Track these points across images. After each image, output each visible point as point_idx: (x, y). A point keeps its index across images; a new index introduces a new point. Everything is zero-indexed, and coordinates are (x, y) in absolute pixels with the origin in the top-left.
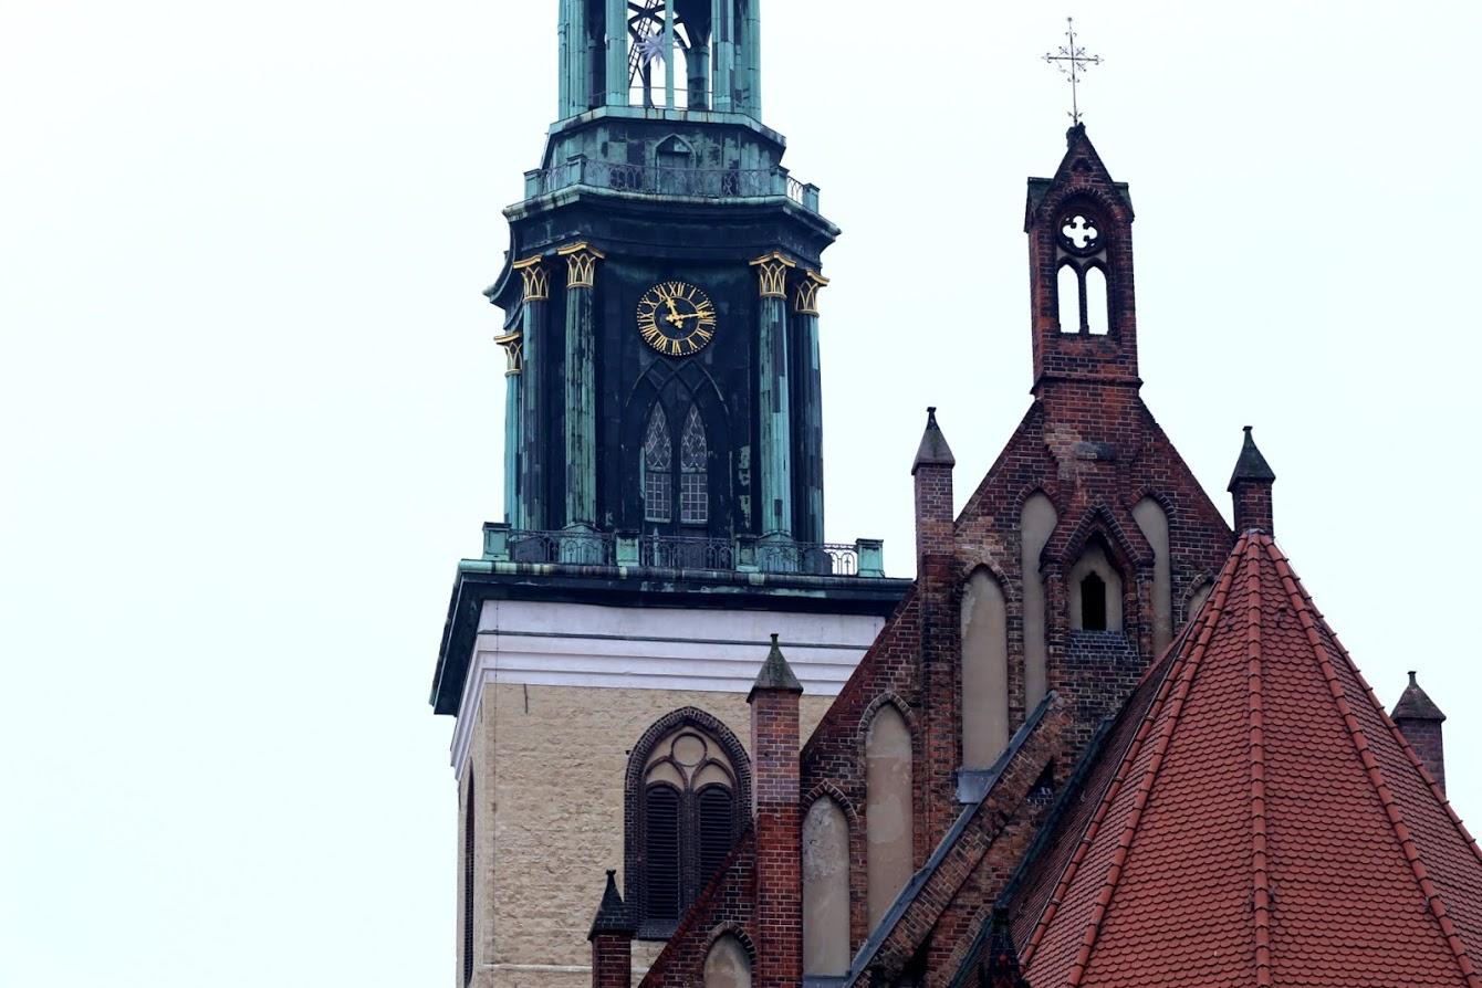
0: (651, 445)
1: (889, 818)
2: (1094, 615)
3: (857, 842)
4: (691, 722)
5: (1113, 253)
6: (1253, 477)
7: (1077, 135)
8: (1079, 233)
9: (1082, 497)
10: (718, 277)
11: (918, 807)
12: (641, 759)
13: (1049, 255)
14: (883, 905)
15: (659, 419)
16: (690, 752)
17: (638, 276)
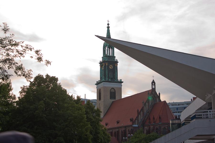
0: (110, 73)
1: (147, 107)
2: (154, 99)
3: (146, 107)
4: (113, 88)
5: (155, 85)
6: (159, 94)
7: (153, 80)
8: (153, 84)
9: (154, 95)
10: (113, 65)
11: (148, 106)
12: (110, 91)
13: (152, 85)
14: (147, 109)
15: (110, 72)
16: (113, 90)
17: (109, 64)
